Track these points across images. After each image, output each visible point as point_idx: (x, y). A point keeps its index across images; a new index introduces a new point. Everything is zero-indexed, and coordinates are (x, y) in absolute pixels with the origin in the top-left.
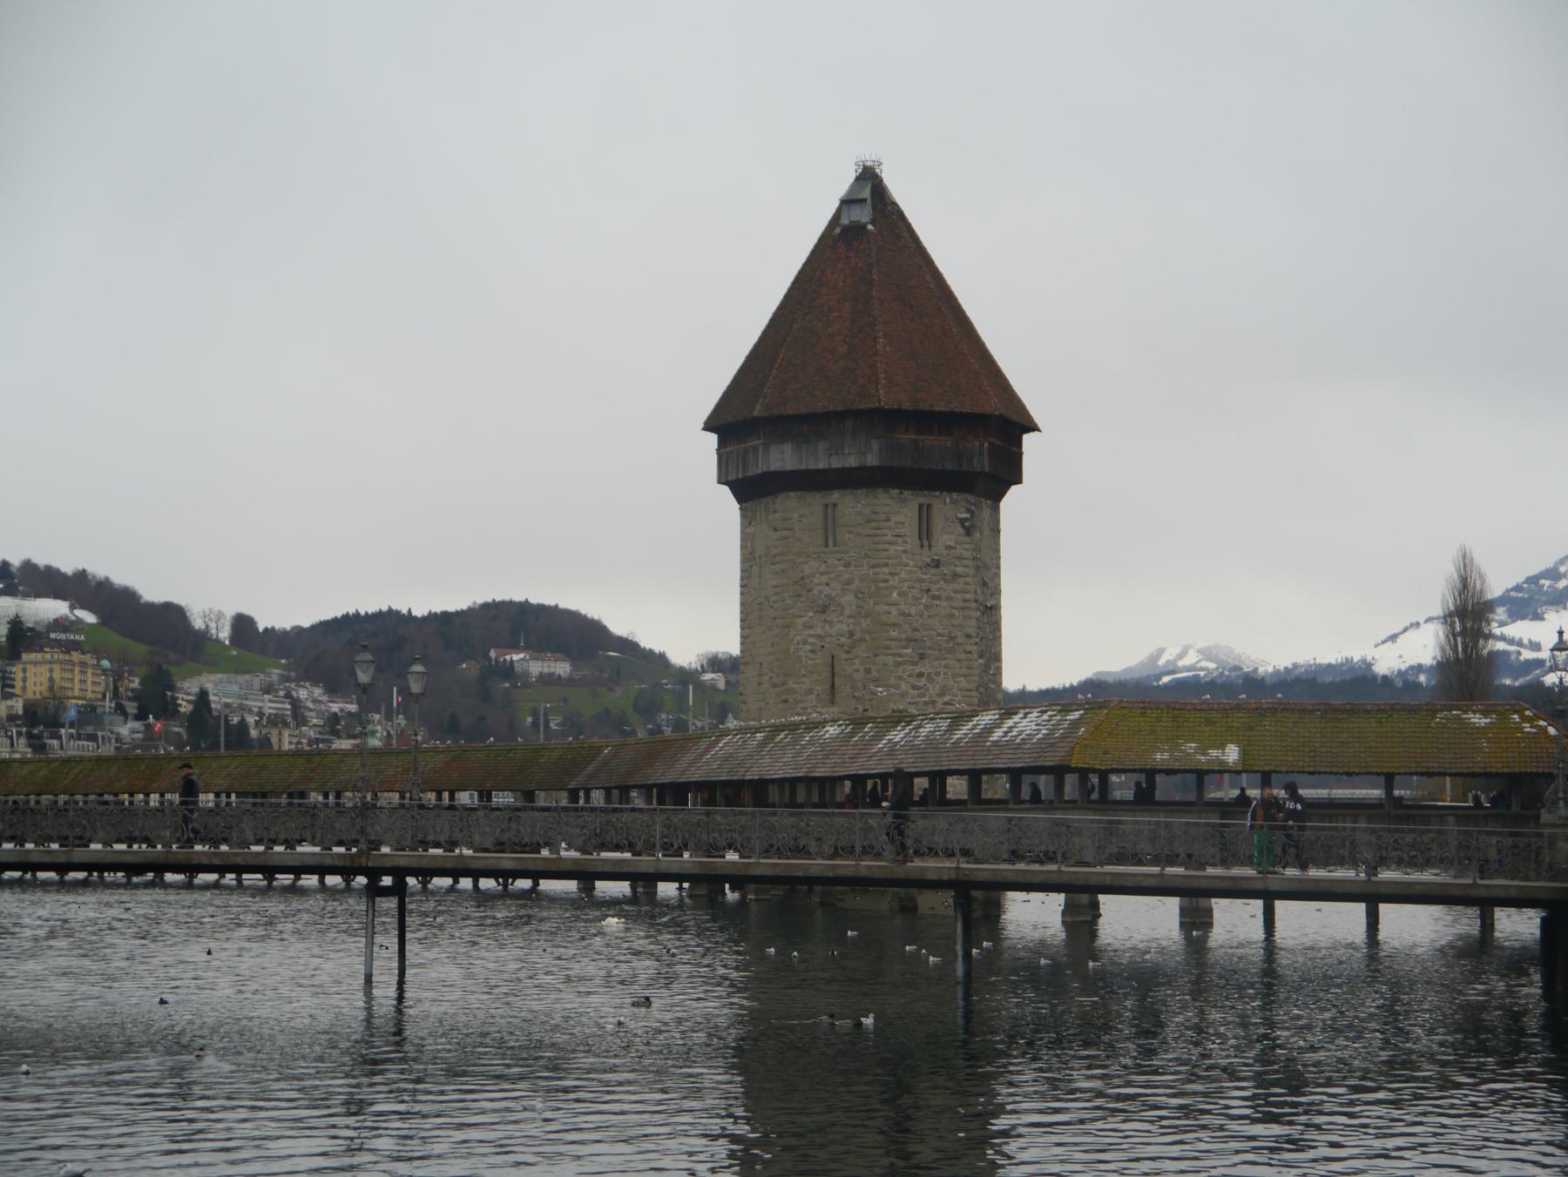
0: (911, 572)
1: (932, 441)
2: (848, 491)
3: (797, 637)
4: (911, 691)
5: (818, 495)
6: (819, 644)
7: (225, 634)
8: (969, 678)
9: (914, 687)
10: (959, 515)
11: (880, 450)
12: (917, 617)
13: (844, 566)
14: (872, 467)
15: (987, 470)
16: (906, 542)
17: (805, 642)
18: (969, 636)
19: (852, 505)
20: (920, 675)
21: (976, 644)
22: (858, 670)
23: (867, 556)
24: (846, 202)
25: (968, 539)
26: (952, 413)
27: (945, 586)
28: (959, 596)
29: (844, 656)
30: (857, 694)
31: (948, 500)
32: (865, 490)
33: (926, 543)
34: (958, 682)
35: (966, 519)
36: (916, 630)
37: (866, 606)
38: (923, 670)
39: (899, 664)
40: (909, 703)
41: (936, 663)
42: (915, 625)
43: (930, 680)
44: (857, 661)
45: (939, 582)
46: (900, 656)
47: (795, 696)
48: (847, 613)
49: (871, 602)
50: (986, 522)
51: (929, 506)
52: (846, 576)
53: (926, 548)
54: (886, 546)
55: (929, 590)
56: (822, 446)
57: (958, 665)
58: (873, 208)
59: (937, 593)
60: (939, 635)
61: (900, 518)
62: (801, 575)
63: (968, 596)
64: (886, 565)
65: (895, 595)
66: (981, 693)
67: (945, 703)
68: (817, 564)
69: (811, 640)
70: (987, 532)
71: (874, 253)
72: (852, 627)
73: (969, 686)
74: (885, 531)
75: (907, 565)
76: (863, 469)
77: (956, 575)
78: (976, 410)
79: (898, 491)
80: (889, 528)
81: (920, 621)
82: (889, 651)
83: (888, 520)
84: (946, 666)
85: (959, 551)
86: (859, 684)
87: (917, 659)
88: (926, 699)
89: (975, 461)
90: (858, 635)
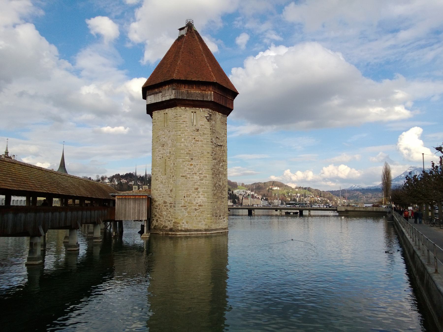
0: (189, 133)
1: (193, 91)
2: (170, 109)
3: (157, 155)
4: (188, 170)
5: (162, 111)
6: (162, 156)
7: (241, 185)
9: (189, 169)
10: (205, 115)
11: (175, 93)
12: (190, 147)
13: (169, 132)
15: (213, 100)
17: (158, 156)
19: (170, 112)
20: (192, 165)
21: (212, 155)
22: (171, 164)
23: (174, 128)
24: (180, 29)
25: (208, 123)
28: (205, 140)
29: (168, 159)
30: (171, 171)
34: (205, 167)
35: (207, 116)
36: (190, 151)
37: (174, 144)
38: (192, 163)
39: (184, 161)
40: (187, 174)
42: (190, 149)
43: (195, 166)
44: (171, 161)
45: (197, 136)
46: (184, 159)
47: (155, 173)
48: (169, 146)
49: (175, 142)
50: (218, 120)
52: (169, 135)
54: (180, 125)
55: (195, 138)
56: (160, 94)
58: (188, 31)
59: (197, 139)
60: (198, 152)
61: (185, 116)
62: (158, 135)
63: (208, 140)
65: (183, 140)
66: (214, 171)
67: (200, 174)
69: (160, 155)
70: (218, 122)
71: (184, 41)
72: (170, 150)
74: (180, 120)
75: (188, 131)
76: (171, 100)
78: (207, 80)
80: (181, 119)
82: (180, 157)
84: (200, 162)
85: (206, 126)
86: (172, 168)
87: (190, 160)
88: (193, 172)
89: (208, 97)
90: (172, 153)
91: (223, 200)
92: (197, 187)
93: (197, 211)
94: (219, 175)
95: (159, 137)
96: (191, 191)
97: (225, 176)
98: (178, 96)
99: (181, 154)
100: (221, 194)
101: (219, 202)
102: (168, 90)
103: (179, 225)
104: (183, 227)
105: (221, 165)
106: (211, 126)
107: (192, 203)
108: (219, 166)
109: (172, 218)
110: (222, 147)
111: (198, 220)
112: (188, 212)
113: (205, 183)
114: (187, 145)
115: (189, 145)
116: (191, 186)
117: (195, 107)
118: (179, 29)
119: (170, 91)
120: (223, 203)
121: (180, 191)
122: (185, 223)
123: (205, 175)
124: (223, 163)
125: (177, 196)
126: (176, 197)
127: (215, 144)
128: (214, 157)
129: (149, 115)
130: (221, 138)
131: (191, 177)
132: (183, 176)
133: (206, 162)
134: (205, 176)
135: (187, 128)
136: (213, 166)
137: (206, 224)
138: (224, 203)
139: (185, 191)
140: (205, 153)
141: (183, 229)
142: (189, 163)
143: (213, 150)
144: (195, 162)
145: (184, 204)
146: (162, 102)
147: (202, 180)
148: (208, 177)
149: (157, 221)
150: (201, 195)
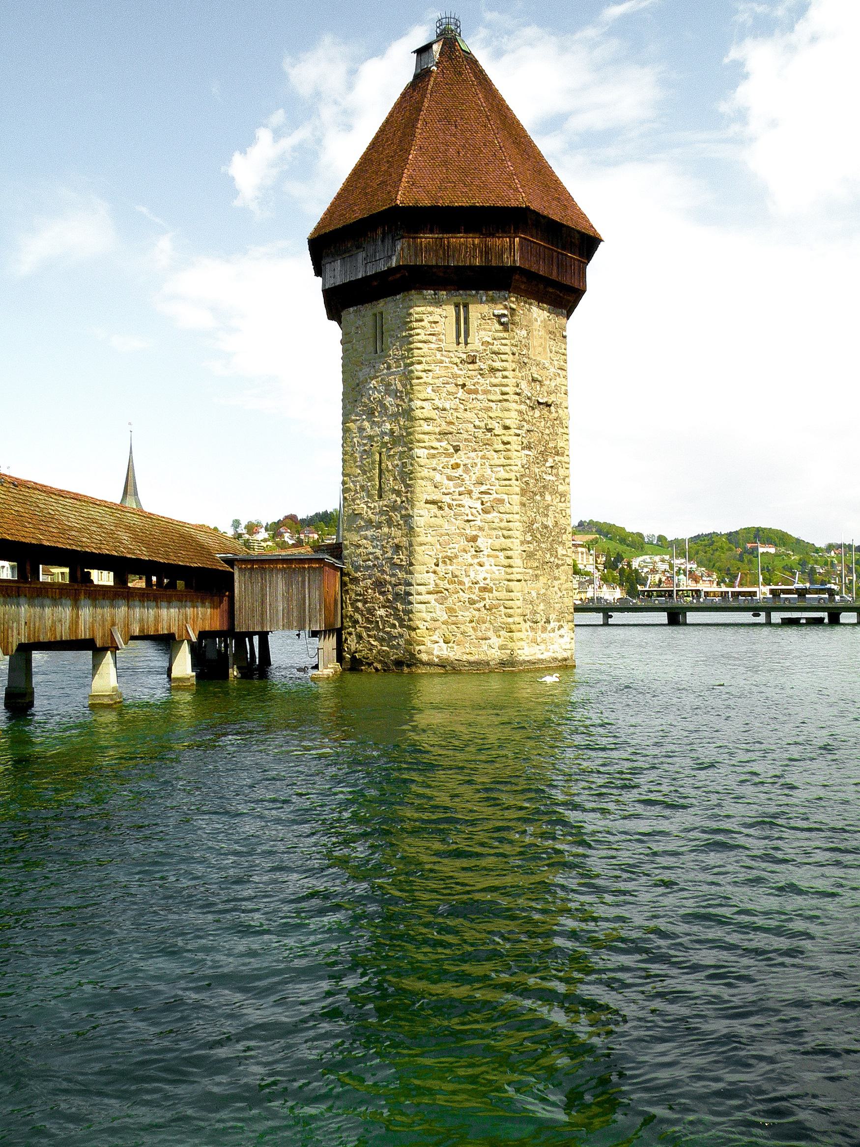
8: (507, 468)
9: (450, 479)
10: (496, 312)
11: (402, 249)
12: (452, 411)
14: (399, 268)
16: (440, 340)
18: (507, 428)
20: (456, 466)
21: (518, 435)
25: (506, 335)
26: (473, 209)
27: (482, 381)
28: (497, 389)
31: (484, 298)
32: (401, 295)
33: (462, 339)
35: (504, 315)
36: (452, 423)
38: (458, 461)
39: (433, 456)
41: (473, 454)
50: (537, 325)
51: (466, 306)
53: (462, 345)
55: (464, 385)
56: (361, 255)
57: (495, 455)
59: (473, 387)
64: (420, 363)
67: (482, 493)
68: (368, 370)
73: (507, 476)
76: (391, 271)
77: (493, 370)
78: (500, 204)
79: (432, 292)
80: (423, 328)
81: (455, 414)
83: (422, 320)
84: (483, 457)
87: (452, 450)
88: (462, 489)
91: (556, 571)
92: (474, 533)
93: (477, 605)
94: (542, 495)
95: (361, 386)
96: (457, 546)
97: (563, 499)
98: (413, 258)
99: (424, 433)
100: (551, 555)
101: (543, 580)
102: (383, 241)
103: (421, 647)
104: (436, 652)
105: (548, 464)
106: (516, 346)
107: (461, 583)
108: (543, 469)
109: (402, 626)
110: (552, 408)
111: (480, 634)
112: (451, 611)
113: (497, 520)
114: (441, 406)
115: (448, 407)
116: (458, 531)
117: (465, 288)
118: (414, 52)
119: (388, 242)
120: (556, 583)
121: (423, 548)
122: (441, 641)
123: (498, 496)
124: (557, 458)
125: (413, 561)
126: (411, 564)
127: (528, 401)
128: (525, 441)
129: (334, 324)
130: (547, 383)
131: (455, 503)
132: (433, 502)
133: (502, 456)
134: (499, 500)
135: (442, 355)
136: (523, 467)
137: (502, 648)
138: (559, 582)
139: (439, 547)
140: (499, 430)
141: (436, 660)
142: (447, 462)
143: (524, 420)
144: (468, 458)
145: (436, 585)
146: (366, 279)
147: (485, 511)
148: (506, 500)
149: (360, 637)
150: (488, 556)
